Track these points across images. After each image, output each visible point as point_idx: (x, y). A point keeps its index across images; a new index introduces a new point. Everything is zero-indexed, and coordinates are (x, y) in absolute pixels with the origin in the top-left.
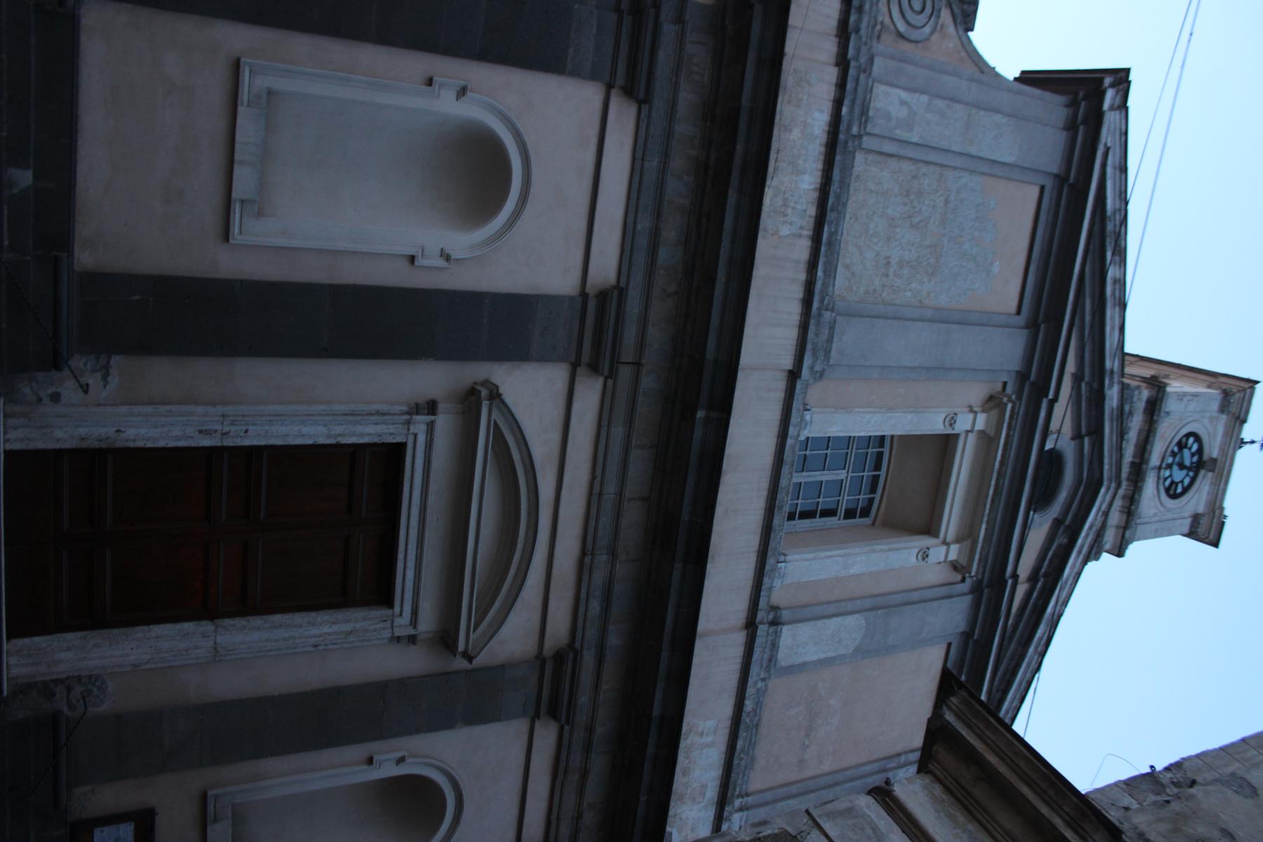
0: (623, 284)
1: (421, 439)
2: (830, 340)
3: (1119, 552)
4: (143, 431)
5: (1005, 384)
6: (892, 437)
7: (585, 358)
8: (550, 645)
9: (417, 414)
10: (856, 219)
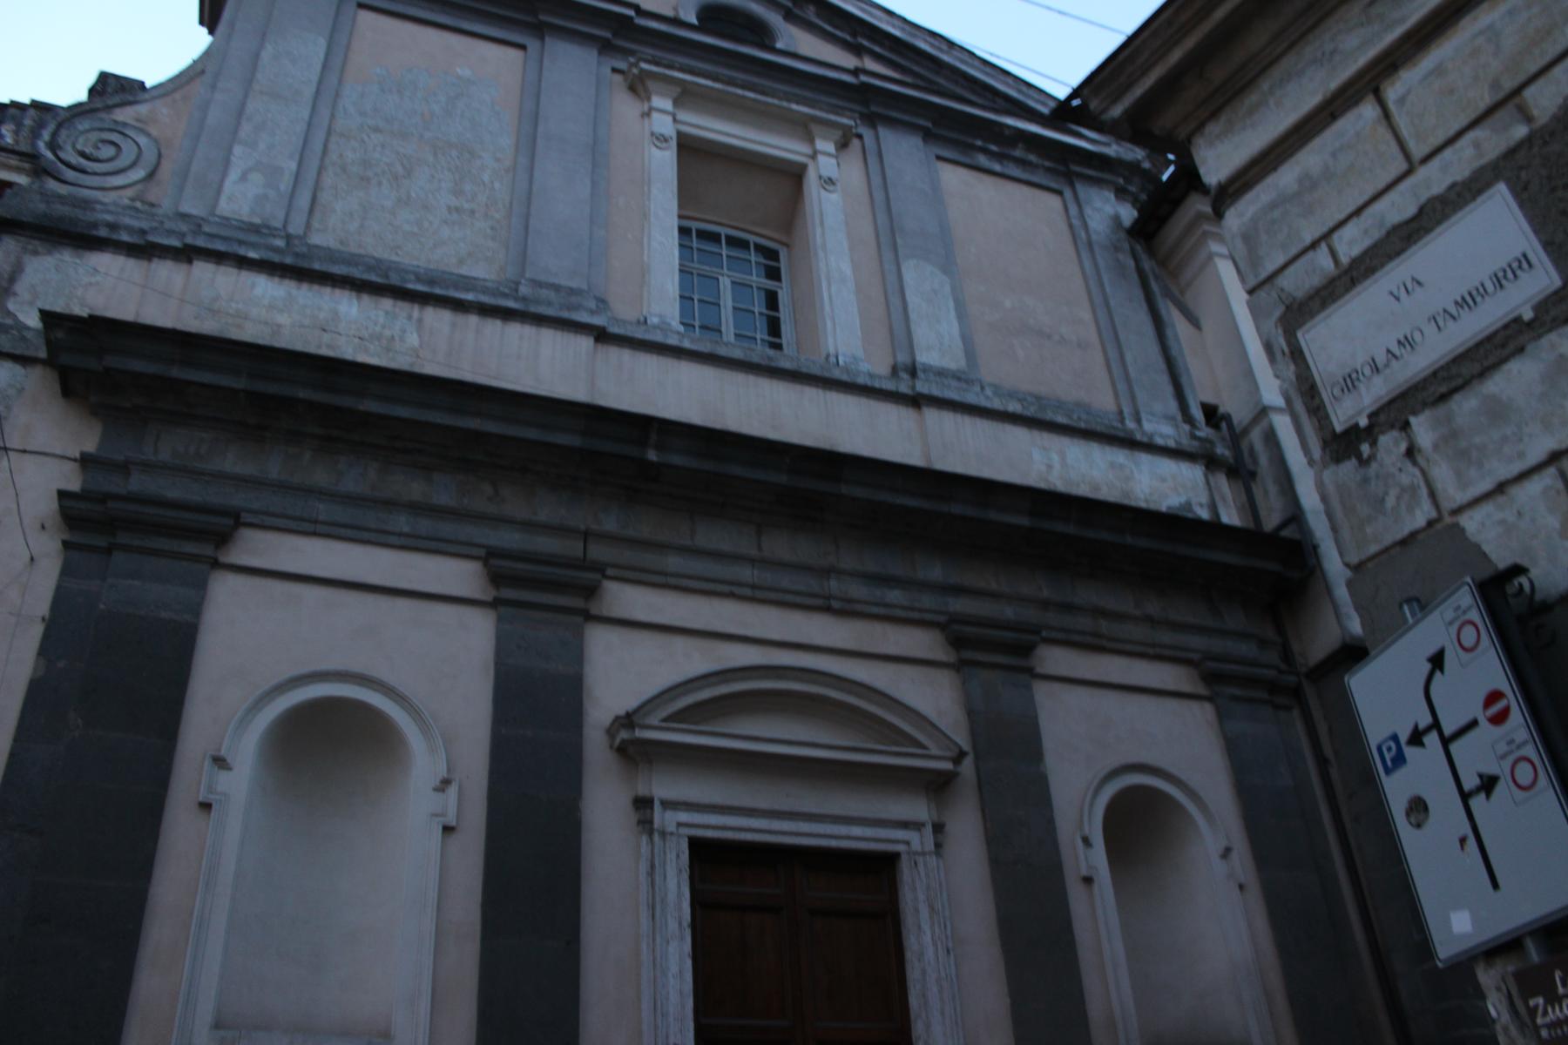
0: (482, 552)
1: (684, 817)
2: (556, 288)
5: (615, 70)
6: (680, 217)
7: (578, 603)
8: (941, 653)
9: (651, 822)
10: (399, 247)
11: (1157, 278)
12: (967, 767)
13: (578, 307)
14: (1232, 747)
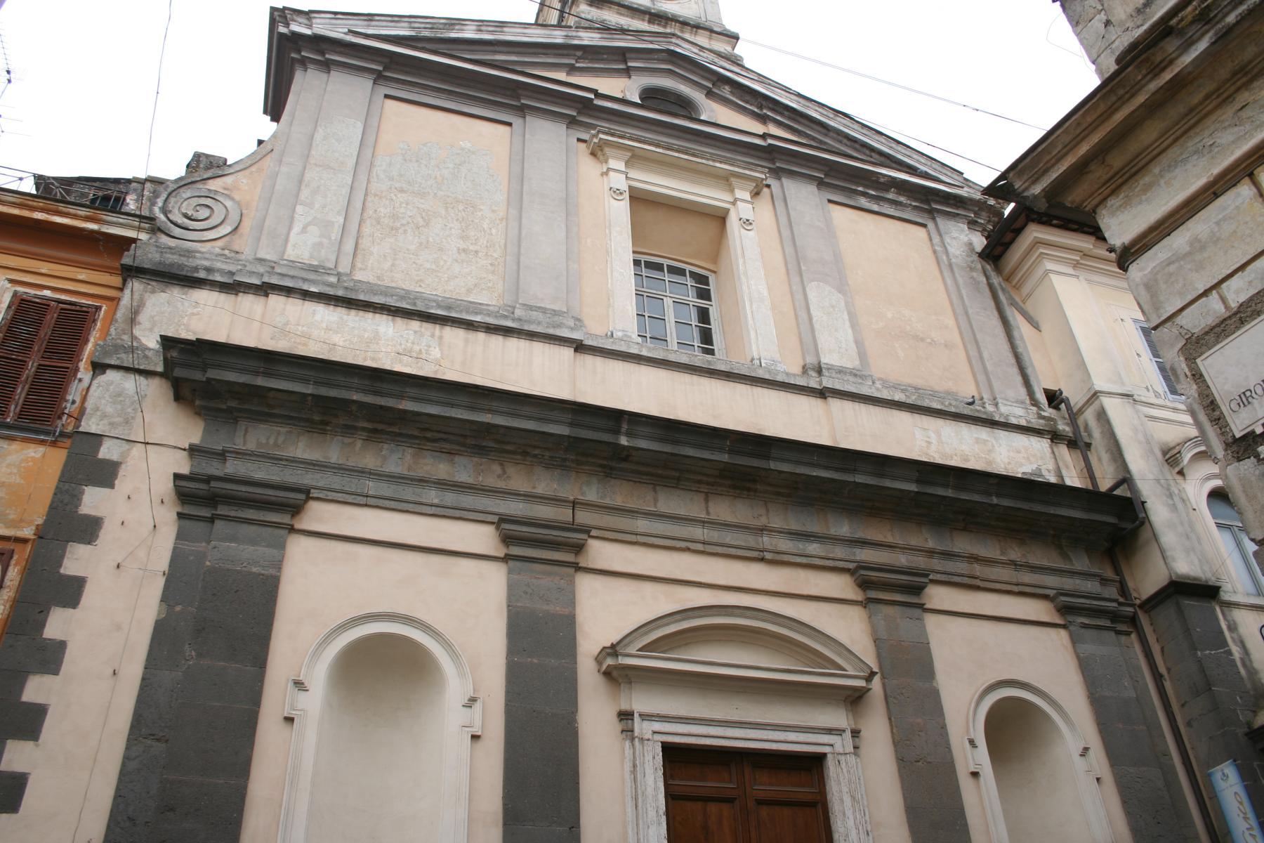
0: (495, 519)
1: (657, 726)
2: (544, 310)
3: (735, 38)
5: (579, 140)
7: (570, 557)
8: (852, 592)
10: (421, 281)
11: (1003, 290)
12: (876, 682)
13: (559, 326)
14: (1085, 665)
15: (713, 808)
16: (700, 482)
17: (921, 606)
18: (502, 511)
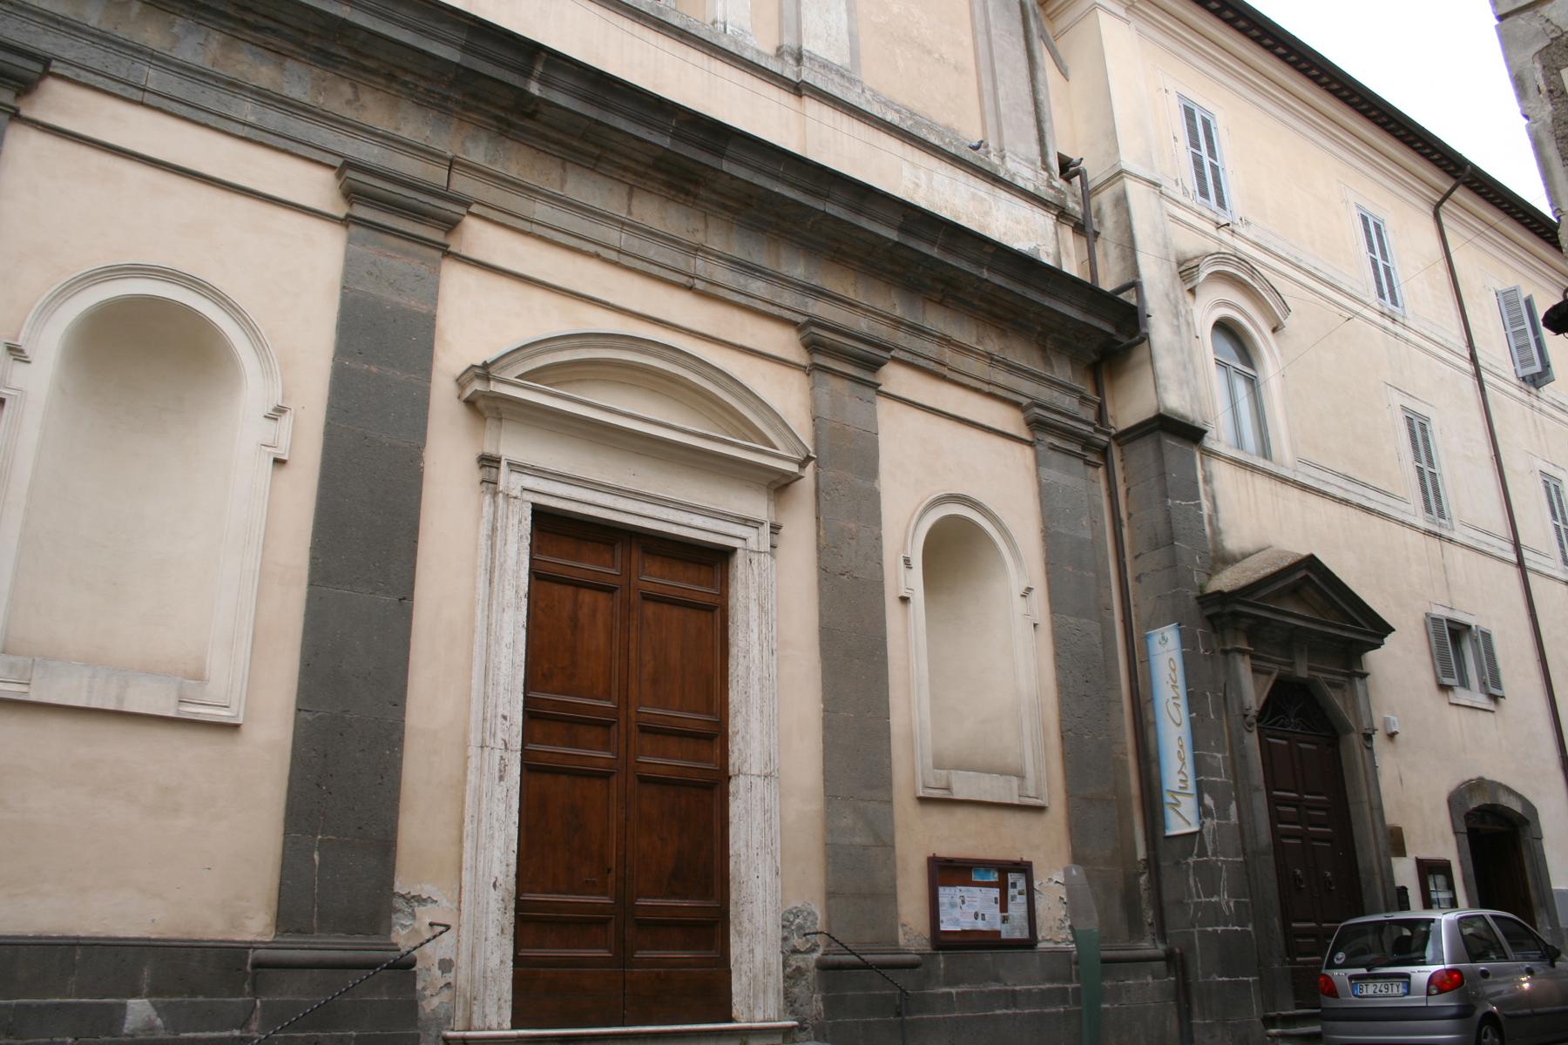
0: (338, 162)
1: (530, 482)
4: (497, 854)
7: (437, 235)
8: (797, 354)
11: (1036, 15)
14: (1045, 493)
15: (586, 596)
16: (625, 169)
17: (875, 386)
18: (347, 152)
